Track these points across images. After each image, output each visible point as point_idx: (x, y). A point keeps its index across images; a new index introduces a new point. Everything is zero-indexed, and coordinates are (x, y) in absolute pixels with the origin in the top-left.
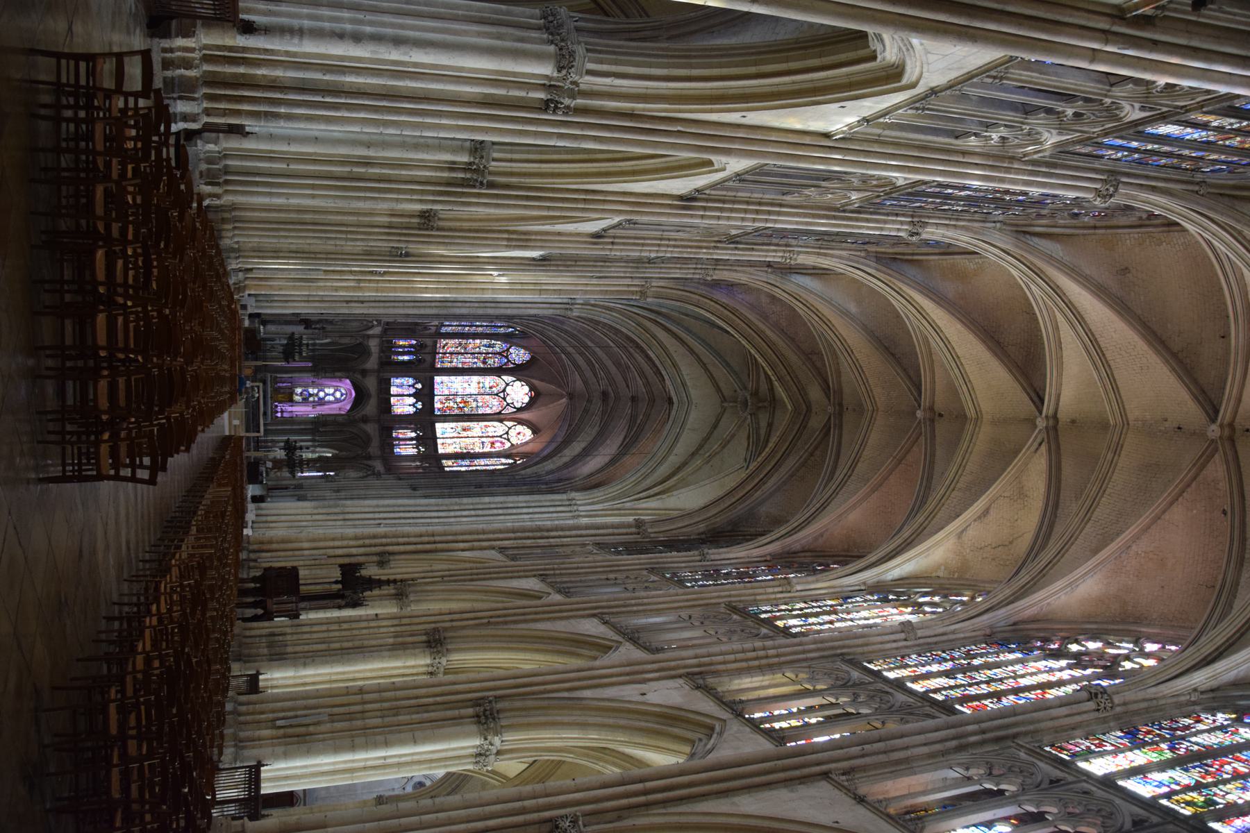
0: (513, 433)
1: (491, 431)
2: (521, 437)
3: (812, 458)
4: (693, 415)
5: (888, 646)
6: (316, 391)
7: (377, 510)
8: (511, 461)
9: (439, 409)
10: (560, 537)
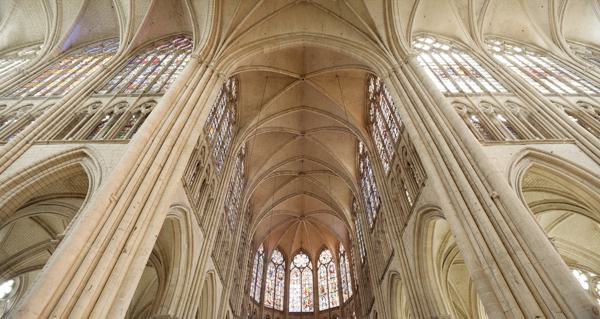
0: (324, 262)
4: (314, 30)
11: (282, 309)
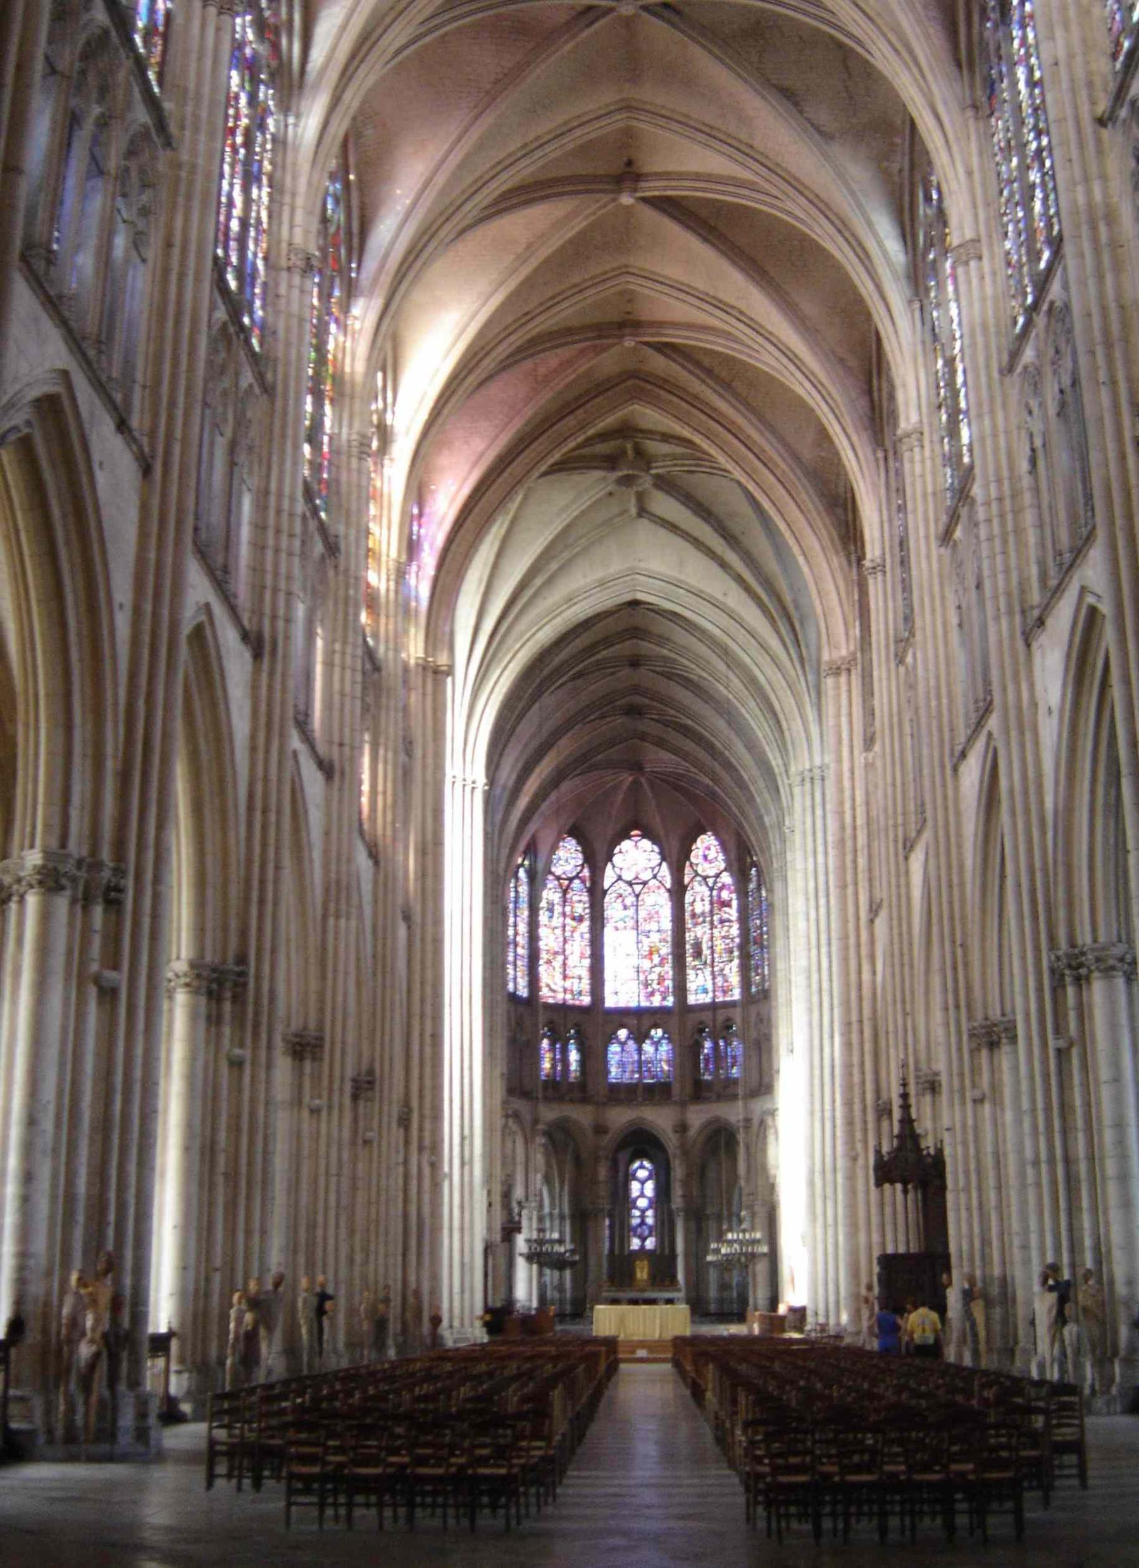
1: (701, 907)
2: (712, 854)
3: (717, 370)
5: (989, 290)
6: (637, 1213)
7: (818, 1115)
8: (753, 871)
9: (664, 999)
10: (854, 808)
11: (586, 1000)
